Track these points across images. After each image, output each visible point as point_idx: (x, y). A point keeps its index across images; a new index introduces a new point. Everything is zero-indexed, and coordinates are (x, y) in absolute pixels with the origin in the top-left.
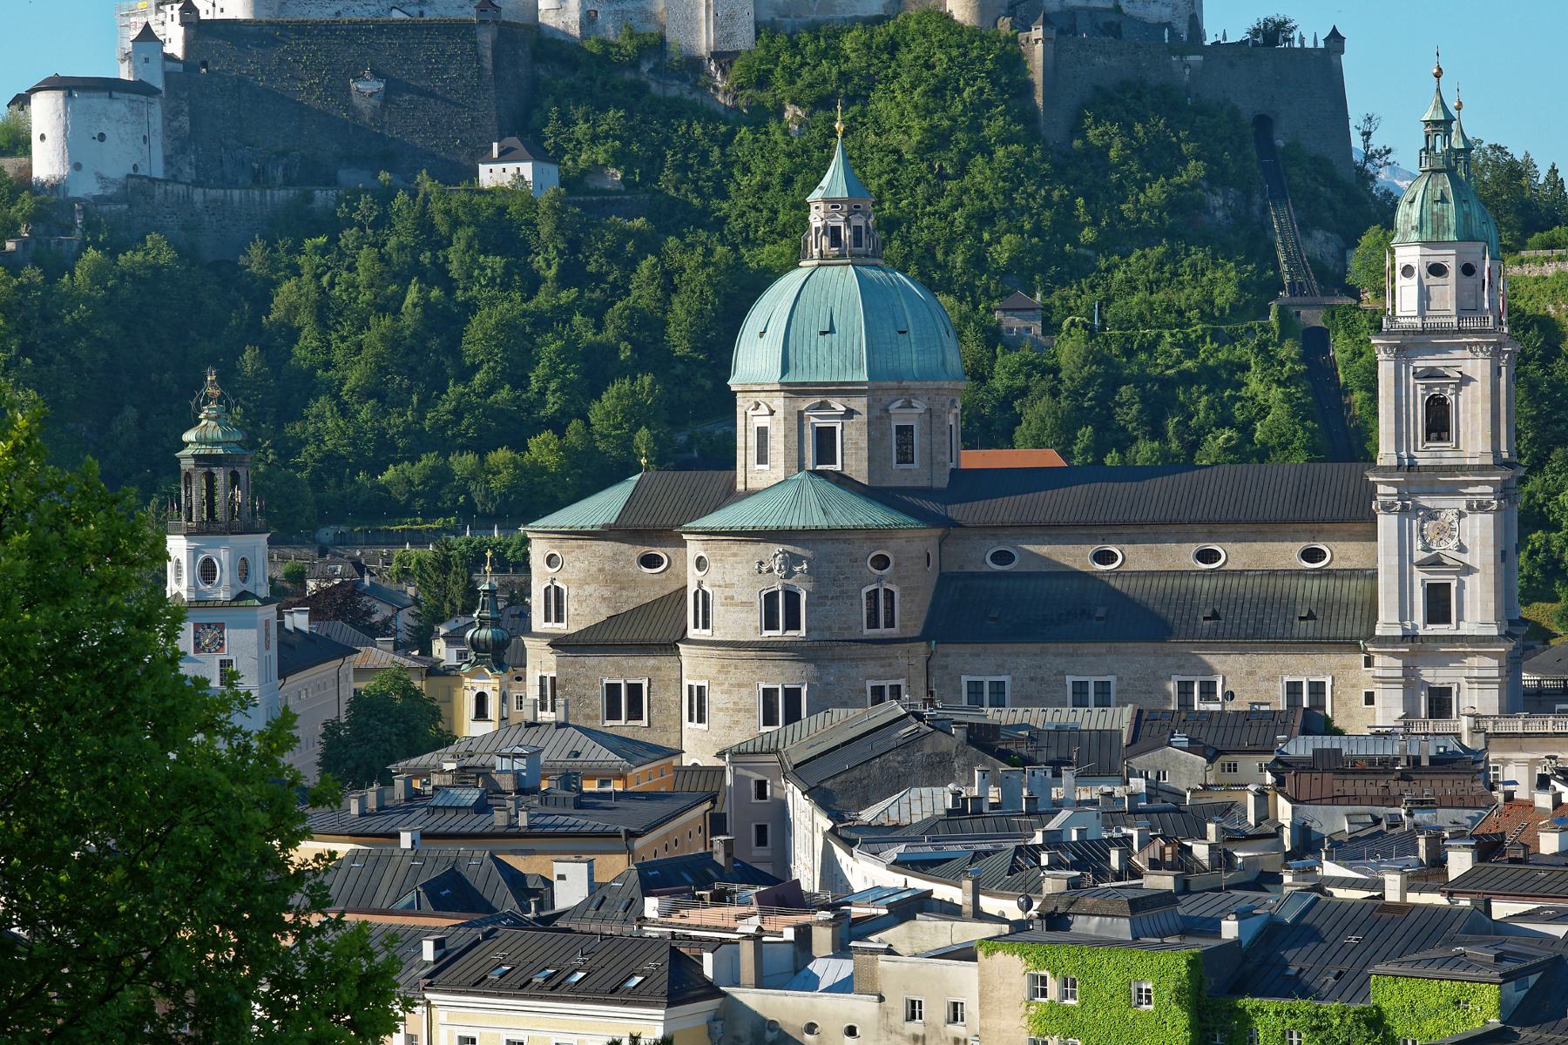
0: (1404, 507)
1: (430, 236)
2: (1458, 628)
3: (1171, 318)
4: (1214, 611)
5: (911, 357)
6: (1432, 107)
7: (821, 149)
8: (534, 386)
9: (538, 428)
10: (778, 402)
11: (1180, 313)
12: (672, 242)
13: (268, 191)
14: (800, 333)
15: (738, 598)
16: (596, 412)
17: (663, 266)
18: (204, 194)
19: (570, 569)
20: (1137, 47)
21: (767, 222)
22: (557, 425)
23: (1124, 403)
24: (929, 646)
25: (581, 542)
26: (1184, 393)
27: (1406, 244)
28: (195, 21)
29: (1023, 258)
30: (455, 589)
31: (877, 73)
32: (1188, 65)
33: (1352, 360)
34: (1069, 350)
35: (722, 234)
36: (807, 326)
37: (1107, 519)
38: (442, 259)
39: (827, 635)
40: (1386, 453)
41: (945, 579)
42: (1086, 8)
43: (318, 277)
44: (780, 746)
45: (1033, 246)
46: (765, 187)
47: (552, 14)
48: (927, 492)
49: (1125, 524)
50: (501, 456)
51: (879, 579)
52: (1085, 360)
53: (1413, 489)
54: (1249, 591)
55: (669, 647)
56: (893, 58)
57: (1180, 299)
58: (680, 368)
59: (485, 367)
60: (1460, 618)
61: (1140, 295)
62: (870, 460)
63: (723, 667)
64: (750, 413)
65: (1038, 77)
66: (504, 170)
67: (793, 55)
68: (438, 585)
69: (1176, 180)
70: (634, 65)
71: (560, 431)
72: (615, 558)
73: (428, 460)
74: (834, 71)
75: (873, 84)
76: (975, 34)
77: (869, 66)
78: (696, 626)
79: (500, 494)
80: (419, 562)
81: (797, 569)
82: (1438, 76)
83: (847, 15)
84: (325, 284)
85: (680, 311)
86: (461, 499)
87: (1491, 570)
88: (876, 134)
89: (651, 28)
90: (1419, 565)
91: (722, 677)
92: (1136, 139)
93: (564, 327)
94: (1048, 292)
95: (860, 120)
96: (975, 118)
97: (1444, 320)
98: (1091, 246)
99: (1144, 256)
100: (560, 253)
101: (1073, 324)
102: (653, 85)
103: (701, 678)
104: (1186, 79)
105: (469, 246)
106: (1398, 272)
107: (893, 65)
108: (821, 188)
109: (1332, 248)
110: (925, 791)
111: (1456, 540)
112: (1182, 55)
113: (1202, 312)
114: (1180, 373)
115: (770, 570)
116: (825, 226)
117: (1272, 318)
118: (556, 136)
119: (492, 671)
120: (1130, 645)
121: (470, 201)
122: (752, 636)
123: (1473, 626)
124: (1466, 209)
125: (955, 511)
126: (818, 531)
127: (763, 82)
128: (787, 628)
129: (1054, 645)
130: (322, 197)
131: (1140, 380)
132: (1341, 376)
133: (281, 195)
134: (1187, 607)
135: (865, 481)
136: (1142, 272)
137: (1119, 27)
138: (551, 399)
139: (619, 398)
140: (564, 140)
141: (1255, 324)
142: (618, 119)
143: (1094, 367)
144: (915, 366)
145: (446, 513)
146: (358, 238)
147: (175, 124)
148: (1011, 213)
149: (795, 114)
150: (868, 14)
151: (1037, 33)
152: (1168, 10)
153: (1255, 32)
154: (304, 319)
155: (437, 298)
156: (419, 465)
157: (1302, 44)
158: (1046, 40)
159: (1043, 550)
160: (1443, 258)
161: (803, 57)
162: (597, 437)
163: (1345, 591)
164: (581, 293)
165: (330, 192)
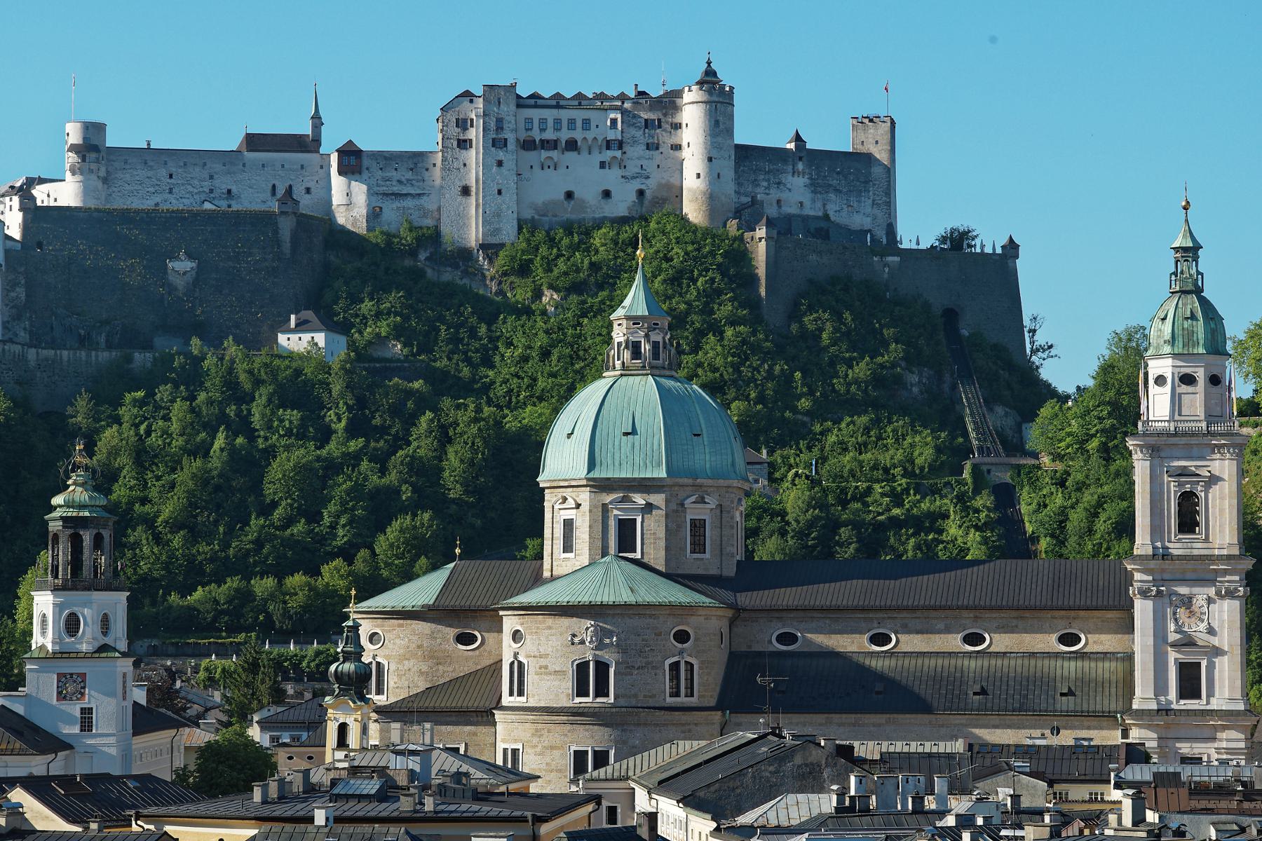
0: (1159, 593)
1: (236, 393)
2: (1208, 703)
3: (879, 474)
4: (982, 687)
5: (704, 458)
6: (1181, 235)
7: (574, 327)
10: (584, 496)
11: (886, 470)
12: (446, 402)
13: (93, 353)
14: (604, 433)
15: (552, 668)
16: (382, 544)
17: (439, 420)
18: (37, 353)
19: (391, 646)
20: (845, 248)
21: (527, 387)
23: (843, 543)
24: (724, 715)
25: (401, 621)
26: (894, 535)
27: (1158, 356)
28: (33, 207)
29: (750, 421)
30: (262, 688)
31: (622, 264)
33: (1037, 511)
34: (793, 498)
35: (488, 397)
37: (883, 604)
38: (245, 412)
39: (634, 703)
40: (1143, 542)
42: (799, 216)
43: (137, 426)
44: (631, 773)
45: (759, 412)
46: (525, 359)
47: (342, 209)
49: (899, 609)
51: (681, 652)
52: (809, 506)
53: (1166, 576)
54: (1012, 670)
55: (484, 716)
57: (885, 459)
60: (1210, 694)
61: (851, 454)
62: (667, 549)
63: (537, 730)
64: (557, 507)
65: (761, 271)
66: (300, 339)
67: (551, 248)
68: (247, 685)
70: (413, 253)
72: (432, 636)
74: (586, 262)
75: (620, 273)
76: (707, 232)
77: (616, 258)
78: (511, 694)
80: (224, 670)
81: (607, 641)
82: (1185, 208)
83: (597, 216)
84: (142, 432)
85: (454, 459)
86: (261, 618)
87: (1237, 651)
89: (429, 222)
90: (1173, 645)
91: (535, 740)
92: (845, 324)
93: (353, 471)
94: (771, 453)
95: (608, 303)
96: (706, 304)
97: (1193, 424)
98: (808, 413)
99: (853, 422)
100: (350, 409)
101: (796, 474)
102: (429, 272)
103: (516, 741)
104: (886, 276)
105: (270, 401)
106: (1151, 382)
108: (623, 307)
109: (1010, 422)
110: (801, 797)
111: (1206, 623)
112: (882, 256)
113: (905, 469)
114: (891, 519)
115: (582, 642)
116: (627, 342)
117: (966, 474)
119: (354, 702)
120: (908, 716)
121: (271, 362)
122: (565, 702)
123: (1221, 702)
124: (1213, 326)
125: (745, 599)
126: (626, 606)
128: (597, 695)
129: (838, 716)
130: (141, 359)
131: (856, 525)
132: (1027, 524)
133: (104, 356)
134: (957, 683)
135: (662, 568)
136: (852, 436)
137: (828, 231)
139: (402, 531)
141: (953, 479)
143: (817, 511)
144: (708, 466)
146: (171, 393)
147: (13, 294)
149: (552, 298)
151: (761, 232)
152: (869, 219)
153: (943, 239)
154: (124, 460)
155: (241, 445)
157: (982, 250)
158: (768, 239)
160: (1193, 369)
161: (559, 249)
163: (1100, 671)
164: (368, 442)
165: (148, 355)
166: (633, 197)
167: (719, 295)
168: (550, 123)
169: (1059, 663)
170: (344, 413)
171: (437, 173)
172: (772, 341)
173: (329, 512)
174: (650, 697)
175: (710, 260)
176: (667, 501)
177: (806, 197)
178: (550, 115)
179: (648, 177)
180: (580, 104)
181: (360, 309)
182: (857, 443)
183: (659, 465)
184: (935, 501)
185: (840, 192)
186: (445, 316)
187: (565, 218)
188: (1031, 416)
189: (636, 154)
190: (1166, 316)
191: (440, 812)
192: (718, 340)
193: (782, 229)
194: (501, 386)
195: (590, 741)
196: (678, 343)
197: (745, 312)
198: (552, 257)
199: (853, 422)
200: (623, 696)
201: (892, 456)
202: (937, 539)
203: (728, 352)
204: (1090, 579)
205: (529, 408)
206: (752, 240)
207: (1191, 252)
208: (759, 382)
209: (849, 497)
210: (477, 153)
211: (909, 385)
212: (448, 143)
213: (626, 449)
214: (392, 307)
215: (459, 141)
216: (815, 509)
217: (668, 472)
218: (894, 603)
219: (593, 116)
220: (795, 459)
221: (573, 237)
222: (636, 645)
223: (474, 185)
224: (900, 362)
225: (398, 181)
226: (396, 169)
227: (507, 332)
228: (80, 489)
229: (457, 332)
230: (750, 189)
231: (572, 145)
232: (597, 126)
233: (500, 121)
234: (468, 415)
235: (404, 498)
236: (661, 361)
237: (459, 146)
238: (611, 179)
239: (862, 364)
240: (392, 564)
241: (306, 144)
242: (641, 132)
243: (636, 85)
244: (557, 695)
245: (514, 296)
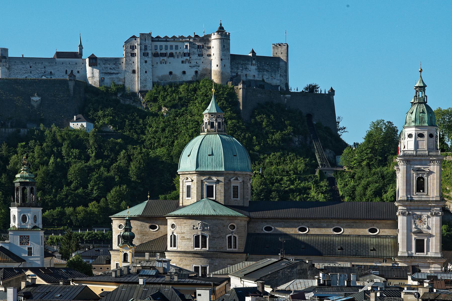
3: (285, 173)
7: (174, 120)
8: (90, 187)
9: (92, 200)
10: (195, 177)
11: (287, 172)
12: (130, 147)
14: (202, 155)
17: (127, 153)
20: (271, 92)
21: (157, 142)
22: (97, 199)
23: (273, 198)
24: (247, 255)
26: (292, 195)
31: (190, 98)
32: (286, 98)
35: (144, 145)
36: (204, 153)
39: (215, 250)
41: (249, 235)
44: (229, 272)
46: (156, 132)
50: (80, 208)
51: (232, 233)
52: (261, 184)
56: (195, 93)
57: (287, 168)
58: (133, 184)
59: (75, 182)
61: (274, 166)
62: (225, 196)
64: (184, 181)
65: (241, 100)
69: (284, 132)
70: (116, 94)
71: (98, 202)
73: (58, 209)
74: (177, 97)
76: (221, 86)
79: (80, 220)
83: (181, 80)
85: (133, 167)
88: (190, 116)
89: (121, 83)
98: (258, 151)
99: (274, 155)
100: (96, 149)
102: (121, 101)
104: (286, 102)
107: (195, 95)
108: (207, 110)
113: (294, 172)
115: (197, 228)
116: (209, 122)
118: (93, 115)
122: (191, 249)
128: (202, 248)
131: (278, 191)
136: (274, 160)
137: (264, 86)
138: (95, 192)
140: (95, 116)
142: (111, 110)
143: (264, 186)
144: (239, 167)
145: (64, 225)
149: (165, 110)
150: (187, 80)
151: (240, 86)
152: (279, 81)
156: (56, 211)
158: (243, 88)
161: (167, 93)
162: (110, 204)
164: (102, 162)
166: (194, 73)
168: (164, 47)
170: (94, 150)
171: (124, 65)
172: (245, 125)
175: (222, 96)
176: (225, 179)
177: (256, 73)
178: (163, 44)
179: (199, 66)
180: (174, 40)
181: (98, 114)
182: (276, 162)
183: (222, 166)
185: (269, 71)
186: (127, 117)
187: (169, 81)
189: (195, 58)
191: (179, 281)
193: (248, 85)
194: (148, 141)
195: (200, 263)
197: (235, 115)
199: (274, 155)
200: (212, 248)
203: (229, 129)
205: (159, 149)
206: (237, 89)
207: (422, 88)
208: (240, 140)
210: (138, 58)
211: (294, 141)
212: (127, 55)
213: (210, 160)
214: (109, 113)
215: (131, 54)
216: (263, 186)
217: (225, 169)
219: (179, 44)
220: (254, 168)
221: (172, 88)
223: (137, 69)
224: (291, 133)
225: (110, 68)
226: (109, 64)
227: (150, 122)
228: (25, 172)
229: (132, 122)
230: (236, 71)
231: (171, 55)
232: (180, 48)
233: (146, 46)
235: (116, 180)
237: (131, 56)
238: (186, 67)
239: (278, 134)
241: (77, 55)
242: (196, 50)
243: (194, 33)
244: (188, 247)
245: (152, 109)
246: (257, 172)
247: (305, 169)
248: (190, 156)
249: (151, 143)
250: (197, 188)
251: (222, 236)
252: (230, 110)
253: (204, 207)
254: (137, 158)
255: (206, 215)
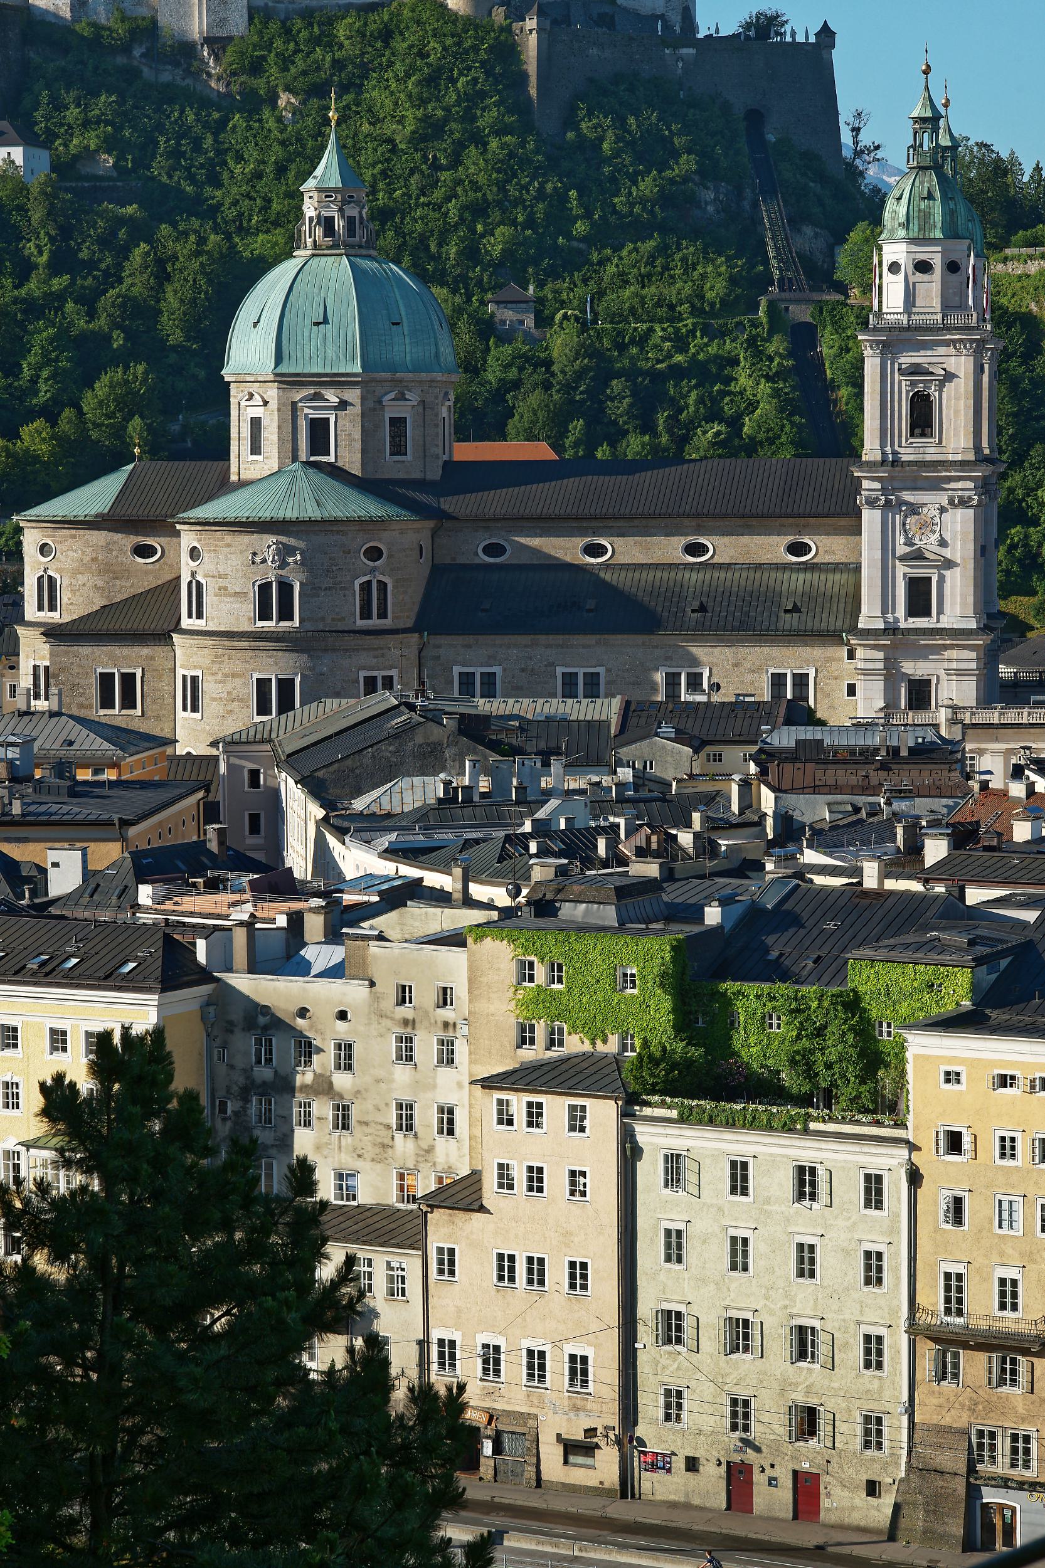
2: (938, 621)
3: (662, 312)
5: (404, 349)
6: (920, 104)
8: (26, 373)
9: (30, 416)
10: (272, 393)
11: (671, 307)
12: (165, 229)
14: (293, 323)
16: (89, 402)
17: (155, 254)
21: (260, 211)
22: (50, 414)
23: (615, 397)
24: (422, 637)
25: (73, 532)
26: (675, 387)
27: (892, 240)
32: (680, 58)
35: (215, 222)
36: (301, 316)
39: (321, 627)
40: (871, 449)
41: (437, 571)
44: (274, 735)
45: (526, 238)
46: (258, 175)
48: (421, 484)
51: (372, 571)
52: (577, 354)
53: (896, 484)
54: (735, 583)
56: (387, 45)
57: (671, 294)
58: (173, 358)
60: (940, 612)
61: (632, 288)
62: (364, 451)
64: (243, 403)
65: (532, 68)
70: (126, 50)
71: (53, 420)
72: (108, 548)
74: (328, 58)
75: (367, 72)
76: (469, 23)
78: (190, 616)
81: (291, 560)
82: (926, 72)
88: (370, 124)
89: (143, 11)
90: (901, 559)
91: (215, 667)
92: (629, 132)
93: (56, 314)
94: (541, 285)
95: (354, 108)
96: (468, 108)
98: (584, 239)
99: (636, 250)
100: (52, 239)
102: (145, 70)
103: (195, 667)
104: (680, 71)
108: (315, 177)
110: (417, 780)
111: (937, 535)
112: (676, 47)
113: (693, 306)
114: (670, 367)
115: (264, 561)
116: (319, 216)
117: (761, 314)
120: (619, 637)
122: (245, 626)
123: (953, 619)
124: (952, 206)
125: (448, 504)
126: (311, 522)
127: (256, 68)
128: (281, 618)
129: (543, 637)
131: (631, 374)
132: (828, 372)
136: (634, 266)
137: (613, 17)
138: (43, 387)
139: (112, 386)
141: (745, 319)
142: (110, 104)
143: (586, 361)
144: (408, 358)
148: (506, 204)
149: (288, 102)
151: (531, 23)
153: (748, 26)
159: (535, 542)
161: (296, 44)
163: (829, 584)
167: (483, 99)
169: (787, 575)
170: (46, 245)
173: (29, 364)
174: (339, 620)
175: (472, 56)
176: (363, 399)
181: (64, 117)
182: (640, 275)
183: (353, 358)
184: (725, 342)
187: (303, 5)
188: (841, 239)
190: (902, 195)
191: (28, 815)
192: (481, 153)
196: (435, 157)
198: (290, 52)
199: (636, 250)
201: (679, 290)
202: (723, 391)
203: (493, 168)
204: (824, 482)
205: (261, 237)
208: (528, 203)
209: (627, 340)
213: (317, 340)
214: (102, 114)
218: (610, 511)
222: (323, 564)
229: (178, 144)
234: (188, 247)
235: (115, 346)
236: (357, 238)
239: (648, 180)
240: (102, 424)
244: (237, 619)
246: (570, 312)
247: (728, 295)
248: (260, 325)
249: (241, 214)
250: (279, 427)
251: (340, 582)
252: (497, 104)
253: (290, 493)
254: (185, 268)
255: (291, 522)
